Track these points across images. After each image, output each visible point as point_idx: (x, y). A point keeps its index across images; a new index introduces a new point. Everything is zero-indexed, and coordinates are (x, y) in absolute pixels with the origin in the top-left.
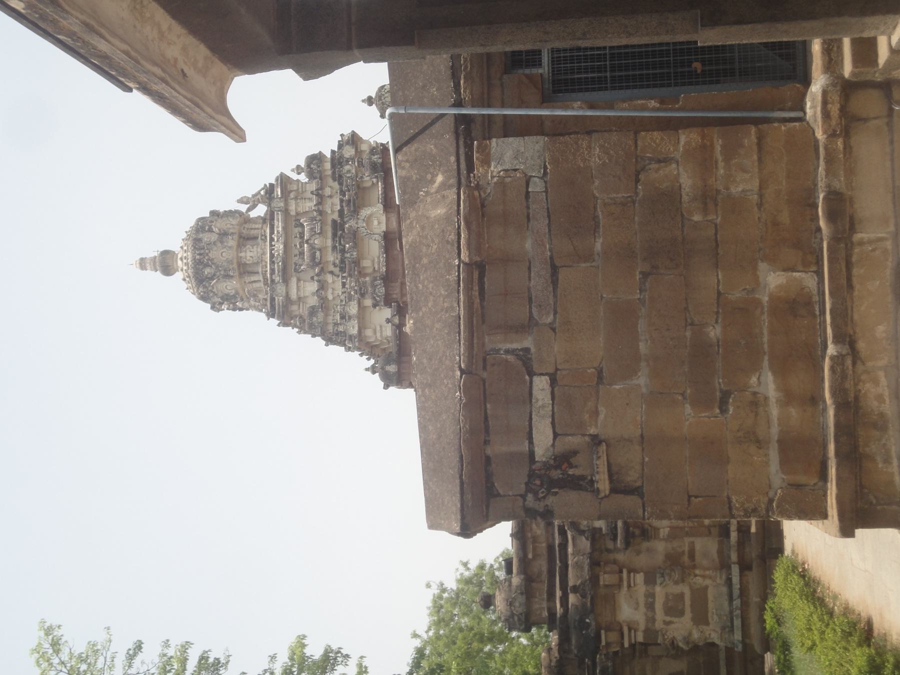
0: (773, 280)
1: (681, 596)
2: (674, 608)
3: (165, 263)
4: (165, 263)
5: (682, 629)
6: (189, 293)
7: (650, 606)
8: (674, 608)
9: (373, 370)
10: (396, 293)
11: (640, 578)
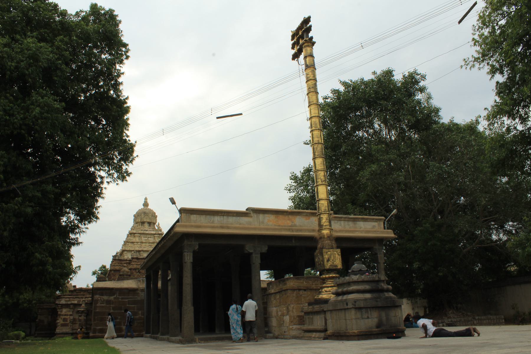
0: (124, 327)
2: (65, 320)
3: (146, 204)
4: (146, 204)
5: (60, 321)
6: (138, 210)
7: (65, 315)
8: (65, 320)
9: (117, 253)
10: (134, 260)
11: (71, 313)
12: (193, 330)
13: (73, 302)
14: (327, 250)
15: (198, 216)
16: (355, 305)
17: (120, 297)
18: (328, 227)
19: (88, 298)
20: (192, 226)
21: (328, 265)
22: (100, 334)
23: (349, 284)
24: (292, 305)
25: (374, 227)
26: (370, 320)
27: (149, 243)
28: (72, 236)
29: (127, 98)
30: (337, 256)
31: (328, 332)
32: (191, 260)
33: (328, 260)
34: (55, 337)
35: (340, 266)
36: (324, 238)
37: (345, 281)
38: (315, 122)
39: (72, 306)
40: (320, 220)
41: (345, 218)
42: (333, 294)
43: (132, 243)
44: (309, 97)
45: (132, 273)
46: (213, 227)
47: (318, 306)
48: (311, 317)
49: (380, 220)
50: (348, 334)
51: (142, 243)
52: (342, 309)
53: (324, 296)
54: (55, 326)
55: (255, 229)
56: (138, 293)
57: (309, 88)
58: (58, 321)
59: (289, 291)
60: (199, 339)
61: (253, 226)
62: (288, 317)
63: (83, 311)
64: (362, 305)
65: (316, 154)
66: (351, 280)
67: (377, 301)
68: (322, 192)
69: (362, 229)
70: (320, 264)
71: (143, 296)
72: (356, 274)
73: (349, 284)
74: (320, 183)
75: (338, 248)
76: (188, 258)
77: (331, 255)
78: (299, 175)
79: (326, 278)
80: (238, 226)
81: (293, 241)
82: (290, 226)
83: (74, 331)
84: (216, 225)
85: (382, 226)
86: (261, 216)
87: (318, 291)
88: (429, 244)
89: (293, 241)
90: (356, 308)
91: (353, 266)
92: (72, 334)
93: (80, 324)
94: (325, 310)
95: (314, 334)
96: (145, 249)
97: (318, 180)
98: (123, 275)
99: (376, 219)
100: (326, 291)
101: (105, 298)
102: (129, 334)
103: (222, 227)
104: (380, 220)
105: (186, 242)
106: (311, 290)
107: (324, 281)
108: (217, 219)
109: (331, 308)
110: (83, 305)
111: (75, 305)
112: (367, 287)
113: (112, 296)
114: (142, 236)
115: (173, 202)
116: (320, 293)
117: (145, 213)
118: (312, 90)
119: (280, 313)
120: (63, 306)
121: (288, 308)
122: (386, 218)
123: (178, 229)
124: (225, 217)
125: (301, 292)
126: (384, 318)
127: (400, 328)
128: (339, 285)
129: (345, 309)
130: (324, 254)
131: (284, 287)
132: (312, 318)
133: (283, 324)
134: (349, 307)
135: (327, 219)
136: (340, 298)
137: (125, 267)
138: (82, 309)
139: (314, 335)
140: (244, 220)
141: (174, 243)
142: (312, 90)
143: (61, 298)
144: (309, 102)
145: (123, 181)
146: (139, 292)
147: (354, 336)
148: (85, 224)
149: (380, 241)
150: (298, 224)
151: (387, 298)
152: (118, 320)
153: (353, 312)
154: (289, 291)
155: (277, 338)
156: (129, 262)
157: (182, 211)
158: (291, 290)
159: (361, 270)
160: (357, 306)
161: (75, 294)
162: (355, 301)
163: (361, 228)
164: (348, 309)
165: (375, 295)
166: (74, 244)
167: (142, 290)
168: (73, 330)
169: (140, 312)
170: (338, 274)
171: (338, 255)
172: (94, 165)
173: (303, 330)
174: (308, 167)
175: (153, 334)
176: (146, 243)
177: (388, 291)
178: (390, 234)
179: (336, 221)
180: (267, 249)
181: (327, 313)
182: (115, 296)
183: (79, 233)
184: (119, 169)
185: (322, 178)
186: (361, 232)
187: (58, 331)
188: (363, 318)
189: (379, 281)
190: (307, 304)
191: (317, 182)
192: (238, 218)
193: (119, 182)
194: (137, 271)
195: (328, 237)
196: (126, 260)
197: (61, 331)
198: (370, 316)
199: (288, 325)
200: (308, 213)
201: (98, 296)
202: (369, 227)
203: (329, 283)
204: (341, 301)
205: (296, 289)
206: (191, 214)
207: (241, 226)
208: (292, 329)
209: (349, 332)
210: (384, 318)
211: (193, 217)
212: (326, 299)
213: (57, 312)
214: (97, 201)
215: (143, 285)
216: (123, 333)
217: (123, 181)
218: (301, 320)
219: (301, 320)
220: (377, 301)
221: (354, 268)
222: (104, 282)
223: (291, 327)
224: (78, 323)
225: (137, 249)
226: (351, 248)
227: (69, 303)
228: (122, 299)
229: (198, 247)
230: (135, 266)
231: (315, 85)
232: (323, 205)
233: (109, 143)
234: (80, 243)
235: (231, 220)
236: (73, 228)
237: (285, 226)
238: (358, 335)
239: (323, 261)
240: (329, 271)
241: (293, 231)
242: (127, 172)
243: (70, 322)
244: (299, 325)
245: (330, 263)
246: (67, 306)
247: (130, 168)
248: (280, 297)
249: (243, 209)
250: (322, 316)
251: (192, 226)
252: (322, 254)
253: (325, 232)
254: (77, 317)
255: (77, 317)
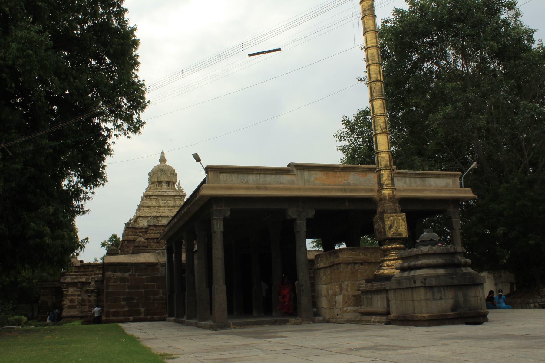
0: (142, 310)
1: (74, 303)
2: (72, 301)
3: (163, 160)
4: (163, 160)
7: (72, 295)
8: (72, 301)
9: (130, 220)
10: (151, 228)
11: (79, 293)
12: (226, 313)
13: (80, 280)
14: (389, 215)
15: (228, 175)
16: (425, 283)
17: (137, 274)
18: (390, 186)
19: (98, 274)
20: (221, 188)
21: (390, 234)
22: (115, 318)
23: (417, 257)
24: (346, 283)
25: (447, 185)
26: (443, 301)
27: (169, 207)
28: (75, 203)
29: (134, 29)
30: (401, 221)
31: (392, 315)
32: (222, 229)
33: (391, 227)
34: (62, 321)
35: (405, 235)
36: (385, 199)
37: (412, 254)
38: (372, 54)
39: (79, 285)
40: (380, 177)
41: (411, 174)
42: (397, 269)
43: (148, 207)
44: (364, 22)
45: (149, 244)
46: (247, 189)
47: (378, 284)
48: (370, 296)
49: (455, 176)
50: (416, 319)
51: (160, 206)
52: (408, 288)
53: (386, 271)
54: (61, 309)
55: (299, 189)
56: (158, 269)
57: (364, 11)
58: (64, 303)
59: (342, 266)
60: (234, 324)
61: (296, 186)
62: (341, 296)
63: (92, 291)
64: (434, 283)
65: (374, 94)
66: (420, 253)
67: (452, 278)
68: (382, 142)
69: (432, 188)
70: (381, 232)
71: (163, 271)
72: (425, 245)
73: (417, 257)
74: (379, 131)
75: (402, 211)
76: (218, 227)
77: (394, 220)
78: (352, 119)
79: (388, 249)
80: (278, 186)
81: (347, 204)
82: (342, 185)
83: (84, 314)
84: (251, 185)
85: (458, 184)
86: (306, 173)
87: (379, 265)
88: (517, 204)
89: (347, 204)
90: (426, 287)
91: (422, 235)
92: (81, 317)
93: (89, 306)
94: (387, 288)
95: (374, 317)
96: (164, 214)
97: (376, 128)
98: (139, 246)
99: (450, 175)
100: (388, 266)
101: (119, 274)
102: (149, 317)
103: (258, 188)
104: (455, 176)
105: (215, 207)
106: (369, 263)
107: (385, 252)
108: (252, 178)
109: (394, 287)
110: (93, 283)
111: (82, 283)
112: (440, 261)
113: (125, 272)
114: (159, 198)
115: (197, 158)
116: (380, 267)
117: (162, 170)
118: (368, 12)
119: (331, 292)
120: (69, 285)
121: (341, 286)
122: (463, 173)
123: (204, 192)
124: (262, 176)
125: (357, 267)
126: (461, 299)
127: (482, 311)
128: (404, 259)
129: (412, 288)
130: (385, 220)
131: (337, 261)
132: (371, 298)
133: (335, 305)
134: (417, 285)
135: (388, 176)
136: (406, 274)
137: (140, 236)
138: (92, 288)
139: (373, 318)
140: (285, 178)
141: (199, 210)
142: (368, 12)
143: (67, 275)
144: (365, 29)
145: (135, 133)
146: (159, 267)
147: (423, 321)
148: (91, 188)
149: (456, 201)
150: (352, 182)
151: (465, 274)
152: (135, 301)
153: (422, 291)
154: (342, 266)
155: (328, 322)
156: (146, 230)
157: (209, 169)
158: (345, 263)
159: (431, 240)
160: (427, 285)
161: (83, 270)
162: (425, 278)
163: (431, 186)
164: (416, 287)
165: (450, 271)
166: (79, 213)
167: (163, 265)
168: (82, 312)
169: (161, 291)
170: (401, 244)
171: (403, 220)
172: (98, 115)
173: (360, 313)
174: (364, 109)
175: (177, 317)
176: (165, 207)
177: (466, 265)
178: (468, 193)
179: (400, 178)
180: (313, 213)
181: (389, 292)
182: (131, 273)
183: (85, 199)
184: (128, 118)
185: (382, 124)
186: (432, 191)
187: (64, 314)
188: (434, 300)
189: (454, 254)
190: (364, 281)
191: (375, 130)
192: (278, 176)
193: (131, 134)
194: (155, 241)
195: (390, 198)
196: (142, 228)
197: (68, 315)
198: (443, 297)
199: (341, 306)
200: (364, 168)
201: (110, 273)
202: (442, 185)
203: (392, 255)
204: (407, 278)
205: (351, 263)
206: (221, 173)
207: (281, 186)
208: (346, 311)
209: (417, 316)
210: (461, 299)
211: (223, 177)
212: (389, 275)
213: (63, 292)
214: (104, 159)
215: (163, 259)
216: (142, 316)
217: (135, 133)
218: (357, 301)
219: (357, 301)
220: (452, 278)
221: (423, 237)
222: (116, 257)
223: (345, 309)
224: (88, 304)
225: (154, 214)
226: (418, 212)
227: (76, 281)
228: (139, 275)
229: (229, 213)
230: (152, 235)
231: (372, 6)
232: (384, 158)
233: (113, 88)
234: (88, 211)
235: (269, 178)
236: (77, 194)
237: (336, 185)
238: (428, 320)
239: (384, 228)
240: (392, 240)
241: (345, 191)
242: (139, 121)
243: (78, 303)
244: (355, 306)
245: (392, 231)
246: (74, 284)
247: (144, 115)
248: (331, 272)
249: (284, 165)
250: (384, 296)
251: (221, 188)
252: (382, 220)
253: (387, 192)
254: (86, 297)
255: (86, 297)
